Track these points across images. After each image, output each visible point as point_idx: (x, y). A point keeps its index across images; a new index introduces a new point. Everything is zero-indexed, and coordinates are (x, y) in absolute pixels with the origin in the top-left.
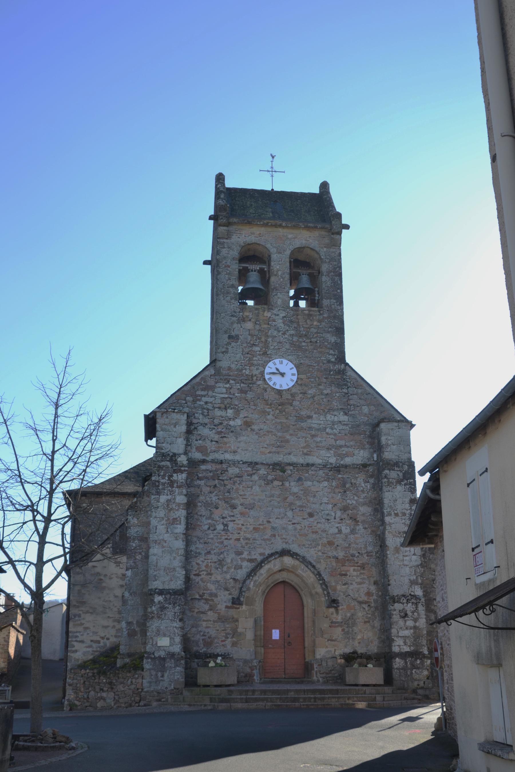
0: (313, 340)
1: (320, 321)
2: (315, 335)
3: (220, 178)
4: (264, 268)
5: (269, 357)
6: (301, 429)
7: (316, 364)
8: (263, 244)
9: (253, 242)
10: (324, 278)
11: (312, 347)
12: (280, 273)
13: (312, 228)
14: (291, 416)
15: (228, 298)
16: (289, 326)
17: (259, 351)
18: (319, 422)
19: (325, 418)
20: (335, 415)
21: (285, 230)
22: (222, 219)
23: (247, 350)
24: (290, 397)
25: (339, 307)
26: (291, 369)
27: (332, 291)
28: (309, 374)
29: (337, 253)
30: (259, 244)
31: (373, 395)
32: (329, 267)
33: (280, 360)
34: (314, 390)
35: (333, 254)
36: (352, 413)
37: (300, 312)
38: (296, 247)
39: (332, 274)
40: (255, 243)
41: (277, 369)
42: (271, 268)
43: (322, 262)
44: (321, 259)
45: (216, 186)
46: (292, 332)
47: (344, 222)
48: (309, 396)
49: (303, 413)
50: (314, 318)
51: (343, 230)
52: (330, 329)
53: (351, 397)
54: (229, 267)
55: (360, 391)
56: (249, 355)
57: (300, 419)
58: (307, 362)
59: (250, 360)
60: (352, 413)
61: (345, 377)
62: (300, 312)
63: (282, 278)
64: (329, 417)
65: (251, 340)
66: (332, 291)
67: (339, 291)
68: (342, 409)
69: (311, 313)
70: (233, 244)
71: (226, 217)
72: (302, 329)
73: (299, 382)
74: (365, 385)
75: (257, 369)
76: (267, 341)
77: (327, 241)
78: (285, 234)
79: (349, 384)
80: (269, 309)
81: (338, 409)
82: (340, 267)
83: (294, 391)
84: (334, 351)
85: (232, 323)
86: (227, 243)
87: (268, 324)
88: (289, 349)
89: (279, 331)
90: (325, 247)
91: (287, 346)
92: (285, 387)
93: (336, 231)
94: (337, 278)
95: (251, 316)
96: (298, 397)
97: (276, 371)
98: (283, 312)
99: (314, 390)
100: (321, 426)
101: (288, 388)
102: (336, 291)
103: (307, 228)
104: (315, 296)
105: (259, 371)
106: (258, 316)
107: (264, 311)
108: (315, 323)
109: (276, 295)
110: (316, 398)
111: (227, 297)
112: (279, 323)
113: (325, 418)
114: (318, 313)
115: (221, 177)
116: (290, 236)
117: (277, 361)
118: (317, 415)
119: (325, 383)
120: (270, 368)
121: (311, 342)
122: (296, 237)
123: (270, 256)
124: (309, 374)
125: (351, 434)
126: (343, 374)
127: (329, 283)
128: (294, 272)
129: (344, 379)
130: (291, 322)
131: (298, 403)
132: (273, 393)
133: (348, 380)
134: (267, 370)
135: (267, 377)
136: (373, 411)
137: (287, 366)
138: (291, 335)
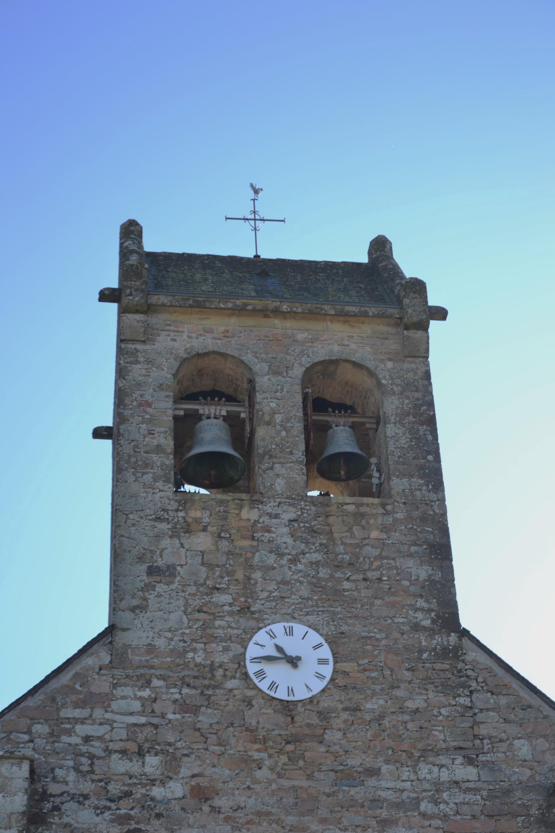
0: (369, 574)
1: (384, 529)
2: (376, 564)
3: (131, 231)
4: (240, 412)
5: (258, 620)
6: (352, 804)
7: (384, 635)
8: (236, 353)
9: (210, 348)
10: (390, 430)
11: (370, 593)
12: (278, 418)
13: (355, 315)
14: (320, 771)
15: (148, 478)
16: (307, 543)
17: (231, 605)
18: (400, 785)
19: (415, 772)
20: (442, 766)
21: (288, 324)
22: (131, 294)
23: (196, 603)
24: (315, 721)
25: (433, 496)
26: (316, 647)
27: (414, 458)
28: (366, 661)
29: (420, 373)
30: (224, 355)
31: (539, 710)
32: (403, 403)
33: (286, 624)
34: (381, 702)
35: (411, 375)
36: (488, 757)
37: (334, 508)
38: (317, 360)
39: (411, 418)
40: (214, 352)
41: (279, 649)
42: (257, 407)
43: (383, 393)
44: (379, 384)
45: (121, 245)
46: (316, 557)
47: (432, 301)
48: (368, 717)
49: (355, 761)
50: (372, 521)
51: (432, 323)
52: (413, 549)
53: (480, 717)
54: (149, 405)
55: (503, 701)
56: (202, 616)
57: (347, 777)
58: (358, 629)
59: (205, 626)
60: (488, 757)
61: (460, 665)
62: (334, 508)
63: (285, 429)
64: (424, 770)
65: (207, 578)
66: (414, 458)
67: (430, 458)
68: (461, 748)
69: (363, 509)
70: (159, 353)
71: (142, 291)
72: (341, 549)
73: (340, 681)
74: (515, 685)
75: (226, 649)
76: (249, 579)
77: (393, 345)
78: (290, 332)
79: (474, 684)
80: (254, 503)
81: (447, 749)
82: (431, 404)
83: (326, 703)
84: (427, 601)
85: (158, 537)
86: (145, 351)
87: (253, 538)
88: (308, 599)
89: (281, 555)
90: (389, 360)
91: (305, 591)
92: (301, 694)
93: (415, 319)
94: (422, 429)
95: (207, 520)
96: (337, 721)
97: (274, 653)
98: (291, 509)
99: (381, 702)
100: (405, 795)
101: (310, 695)
102: (425, 458)
103: (343, 316)
104: (371, 477)
105: (231, 654)
106: (226, 519)
107: (241, 507)
108: (374, 534)
109: (272, 468)
110: (386, 722)
111: (144, 474)
112: (282, 535)
113: (415, 772)
114: (381, 511)
115: (132, 228)
116: (300, 336)
117: (278, 628)
118: (391, 767)
119: (410, 682)
120: (261, 644)
121: (365, 579)
122: (318, 339)
123: (251, 381)
124: (366, 661)
125: (490, 816)
126: (457, 657)
127: (403, 441)
128: (314, 420)
129: (460, 671)
130: (312, 531)
131: (339, 735)
132: (270, 711)
133: (470, 673)
134: (252, 651)
135: (252, 668)
136: (543, 752)
137: (306, 641)
138: (311, 563)
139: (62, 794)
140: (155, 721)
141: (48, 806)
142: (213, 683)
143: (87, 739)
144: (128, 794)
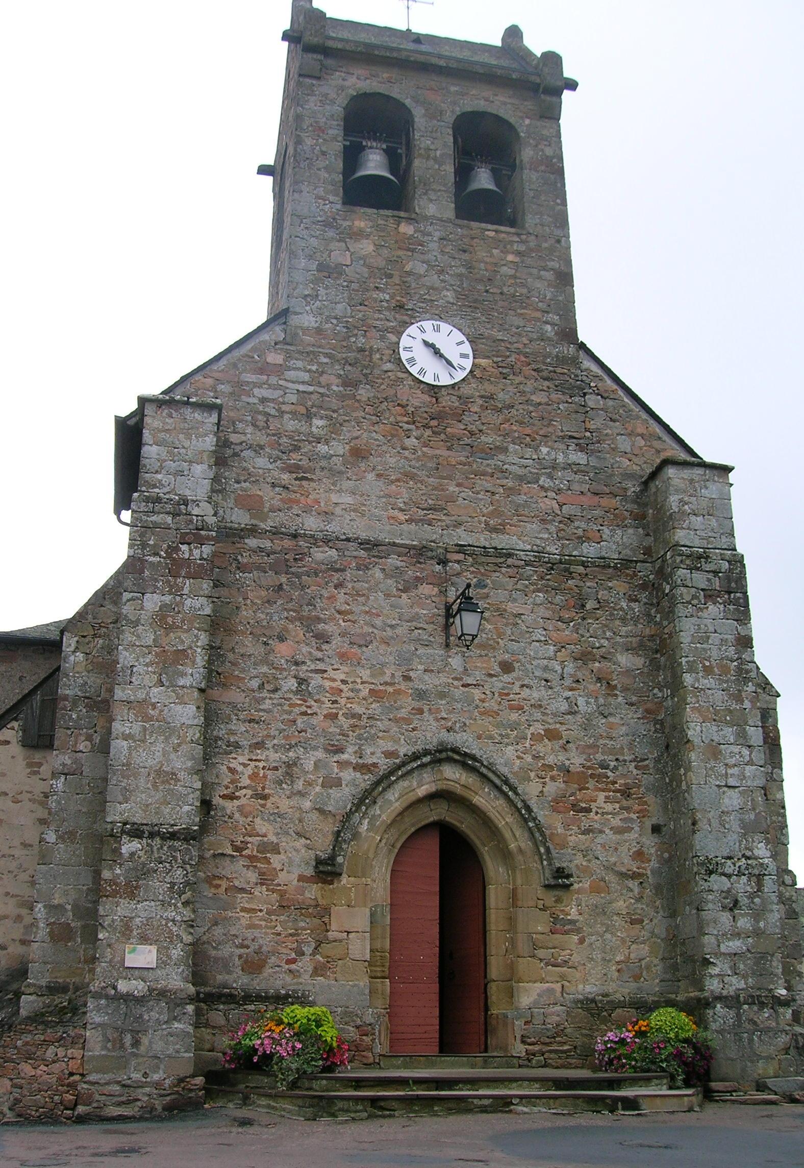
0: (505, 290)
25: (558, 232)
26: (459, 344)
51: (565, 91)
80: (409, 220)
83: (466, 390)
88: (453, 304)
108: (510, 258)
117: (428, 325)
121: (501, 293)
133: (585, 378)
139: (241, 443)
140: (321, 390)
141: (229, 452)
142: (368, 368)
143: (263, 400)
144: (297, 448)
